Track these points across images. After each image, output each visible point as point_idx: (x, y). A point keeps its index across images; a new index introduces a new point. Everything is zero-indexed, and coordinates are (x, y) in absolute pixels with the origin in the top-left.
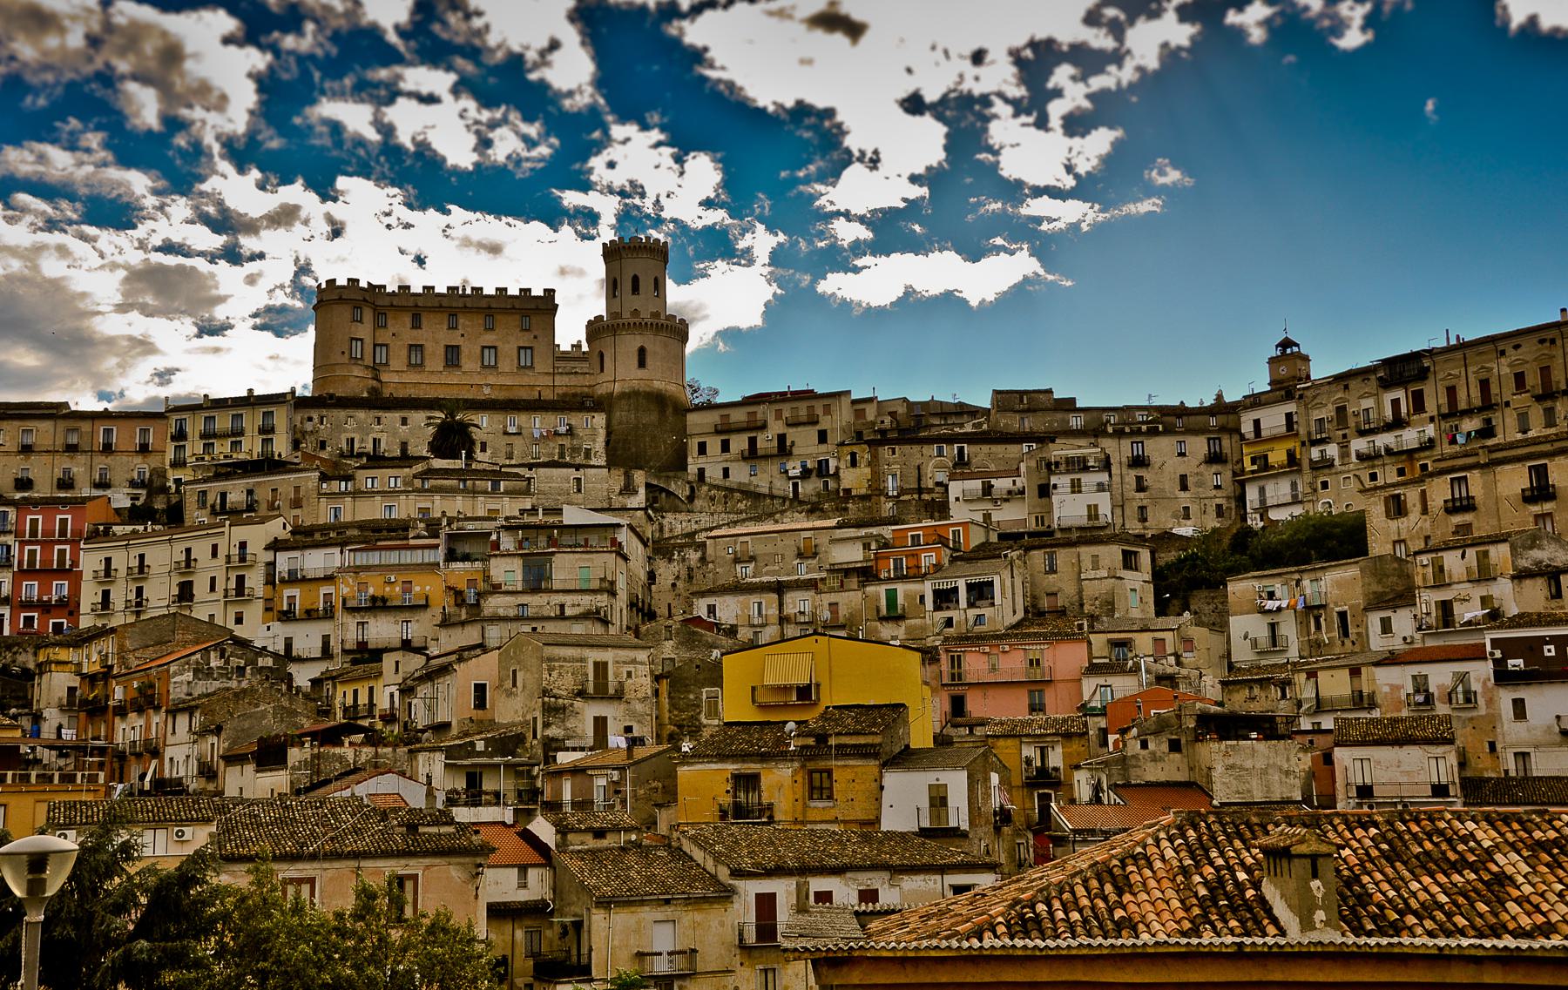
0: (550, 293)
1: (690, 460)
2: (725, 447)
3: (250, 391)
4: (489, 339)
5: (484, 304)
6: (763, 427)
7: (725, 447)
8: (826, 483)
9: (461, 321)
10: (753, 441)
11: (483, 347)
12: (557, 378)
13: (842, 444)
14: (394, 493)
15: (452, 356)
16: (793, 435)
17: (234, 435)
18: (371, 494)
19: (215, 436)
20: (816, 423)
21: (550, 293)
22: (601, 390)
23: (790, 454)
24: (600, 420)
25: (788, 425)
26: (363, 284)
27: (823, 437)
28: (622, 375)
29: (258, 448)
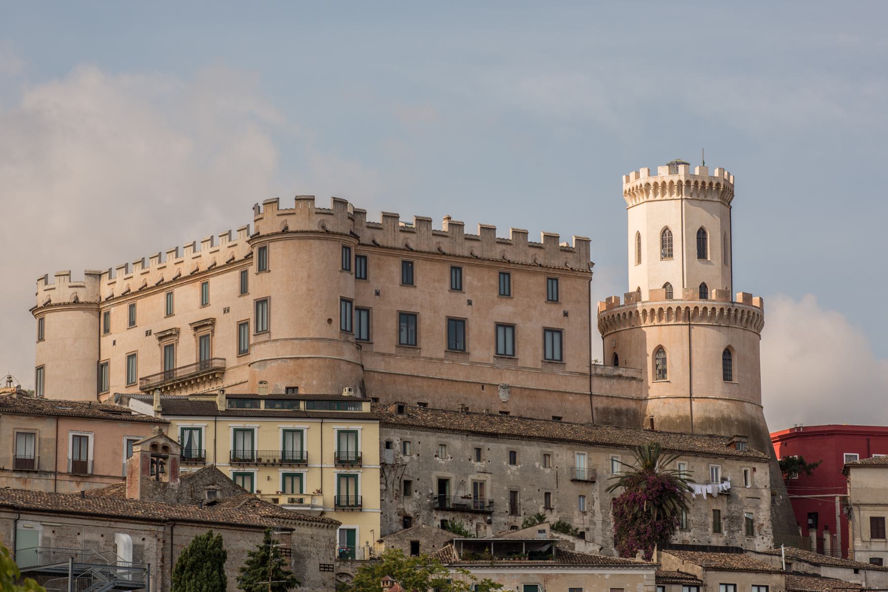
1: (858, 544)
4: (505, 311)
5: (496, 252)
12: (596, 382)
17: (284, 461)
21: (583, 243)
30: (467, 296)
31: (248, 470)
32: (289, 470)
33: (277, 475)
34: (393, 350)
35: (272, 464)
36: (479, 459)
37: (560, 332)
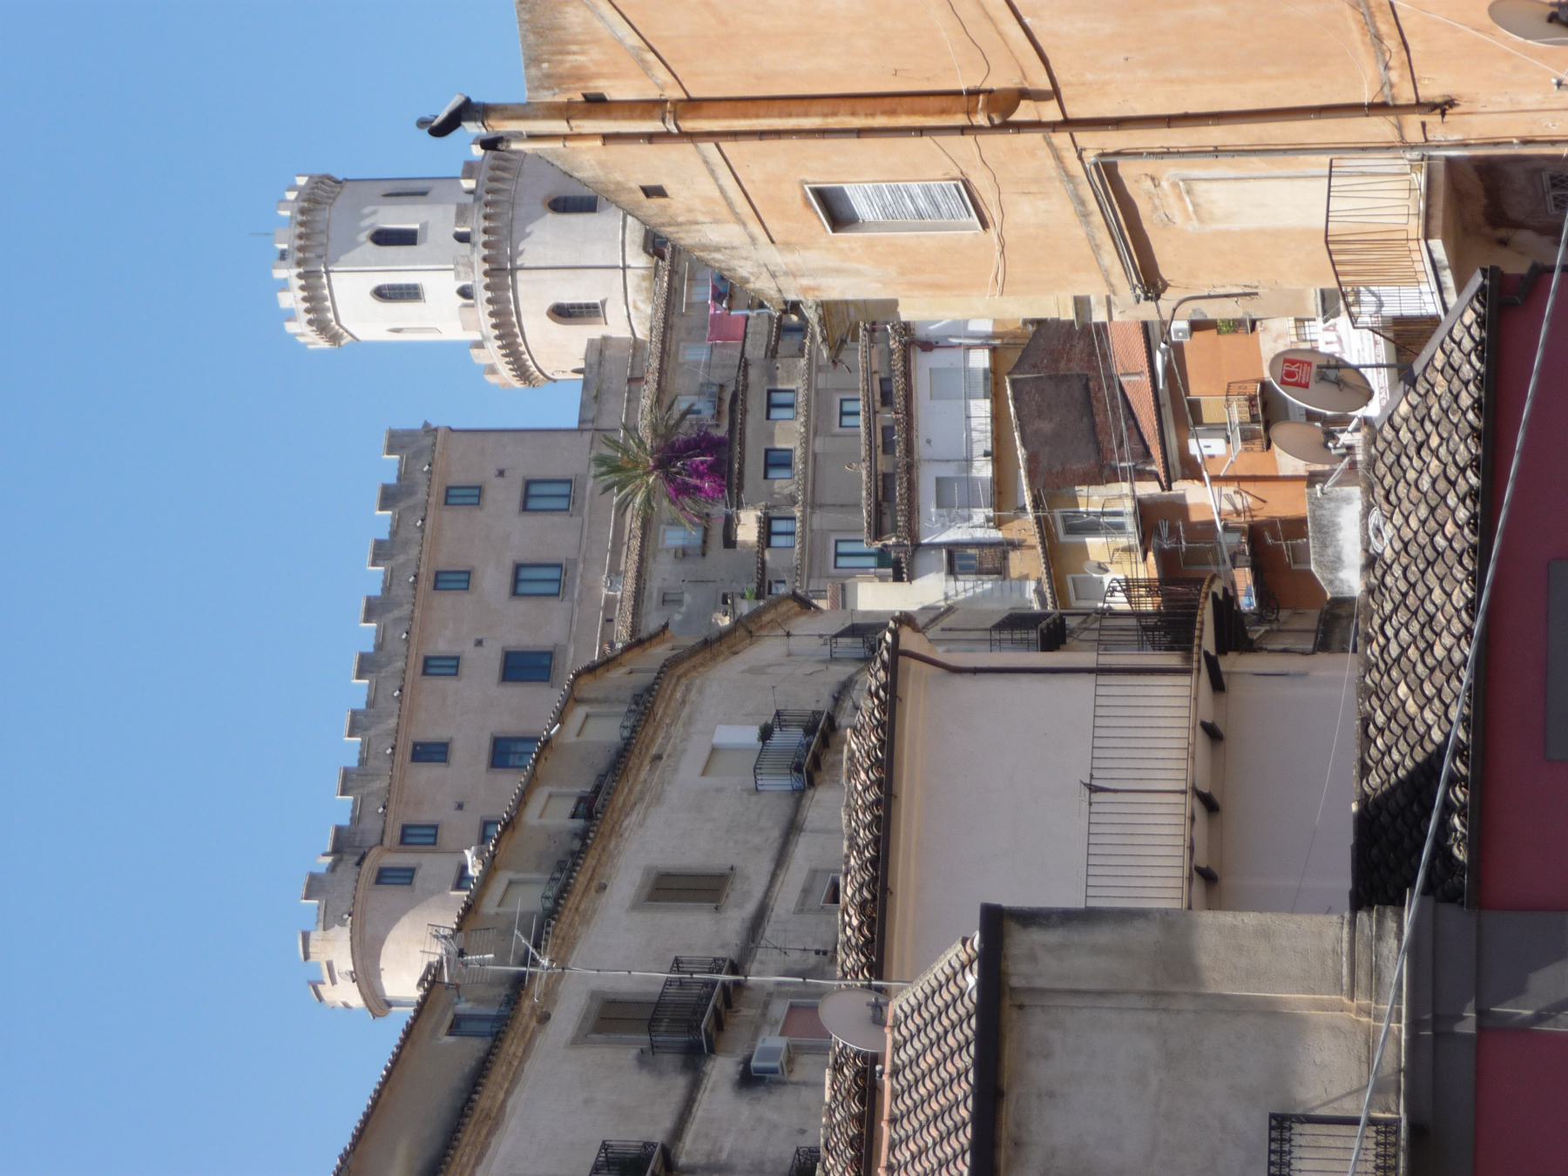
0: (396, 441)
4: (493, 580)
9: (441, 647)
21: (396, 441)
30: (468, 651)
37: (528, 484)
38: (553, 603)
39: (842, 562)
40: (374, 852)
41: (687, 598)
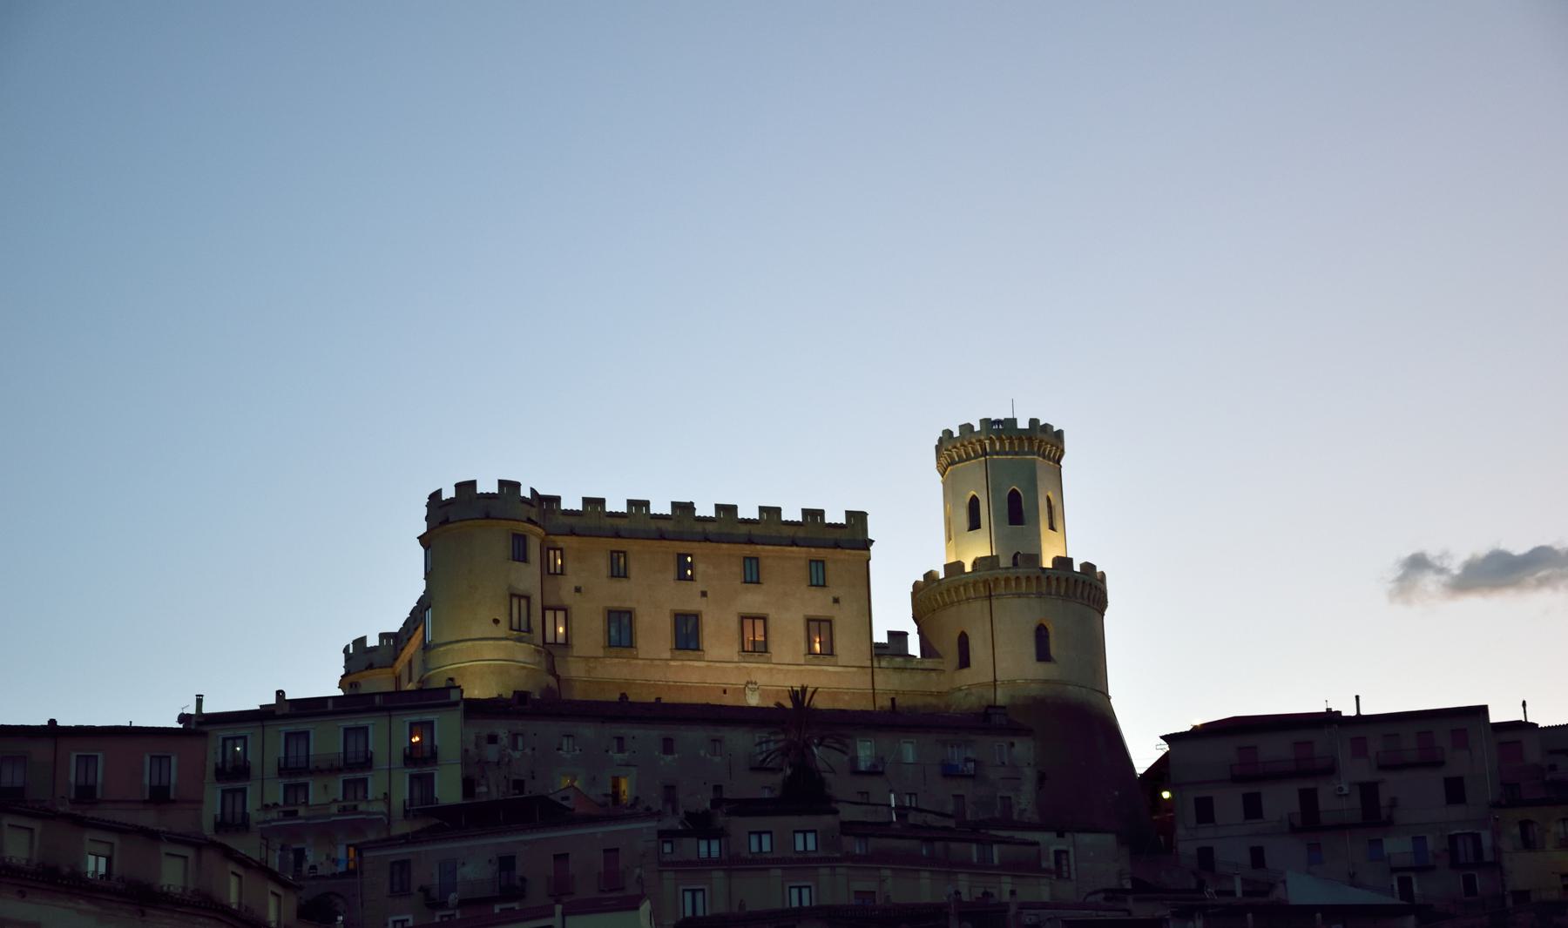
0: (857, 519)
1: (1181, 832)
2: (1253, 807)
3: (280, 694)
6: (1330, 770)
7: (1253, 807)
8: (1469, 884)
10: (1308, 799)
11: (743, 618)
13: (1496, 805)
14: (805, 861)
15: (687, 634)
16: (1393, 786)
17: (349, 766)
18: (760, 863)
19: (305, 770)
20: (1438, 764)
21: (857, 519)
22: (972, 702)
23: (1389, 823)
24: (1023, 749)
25: (1382, 768)
26: (525, 492)
27: (1455, 791)
28: (1005, 663)
29: (402, 793)
31: (301, 780)
32: (350, 776)
33: (336, 786)
34: (600, 653)
35: (333, 770)
36: (621, 749)
37: (829, 621)
38: (737, 647)
39: (688, 896)
40: (539, 530)
41: (717, 759)
